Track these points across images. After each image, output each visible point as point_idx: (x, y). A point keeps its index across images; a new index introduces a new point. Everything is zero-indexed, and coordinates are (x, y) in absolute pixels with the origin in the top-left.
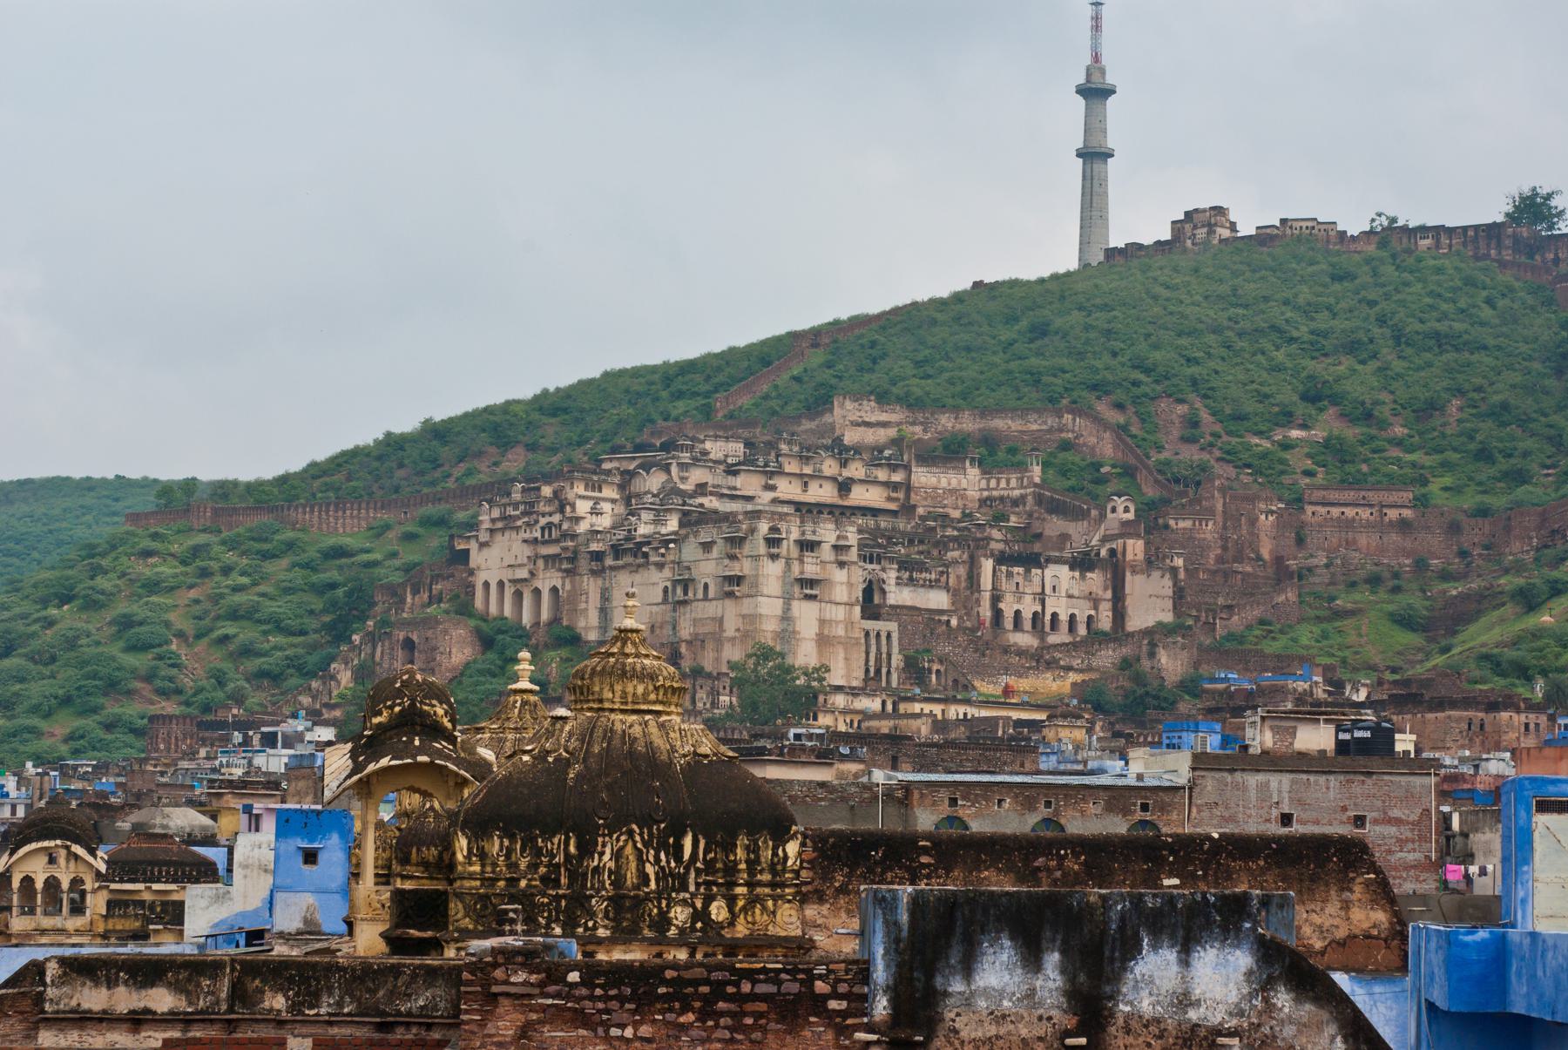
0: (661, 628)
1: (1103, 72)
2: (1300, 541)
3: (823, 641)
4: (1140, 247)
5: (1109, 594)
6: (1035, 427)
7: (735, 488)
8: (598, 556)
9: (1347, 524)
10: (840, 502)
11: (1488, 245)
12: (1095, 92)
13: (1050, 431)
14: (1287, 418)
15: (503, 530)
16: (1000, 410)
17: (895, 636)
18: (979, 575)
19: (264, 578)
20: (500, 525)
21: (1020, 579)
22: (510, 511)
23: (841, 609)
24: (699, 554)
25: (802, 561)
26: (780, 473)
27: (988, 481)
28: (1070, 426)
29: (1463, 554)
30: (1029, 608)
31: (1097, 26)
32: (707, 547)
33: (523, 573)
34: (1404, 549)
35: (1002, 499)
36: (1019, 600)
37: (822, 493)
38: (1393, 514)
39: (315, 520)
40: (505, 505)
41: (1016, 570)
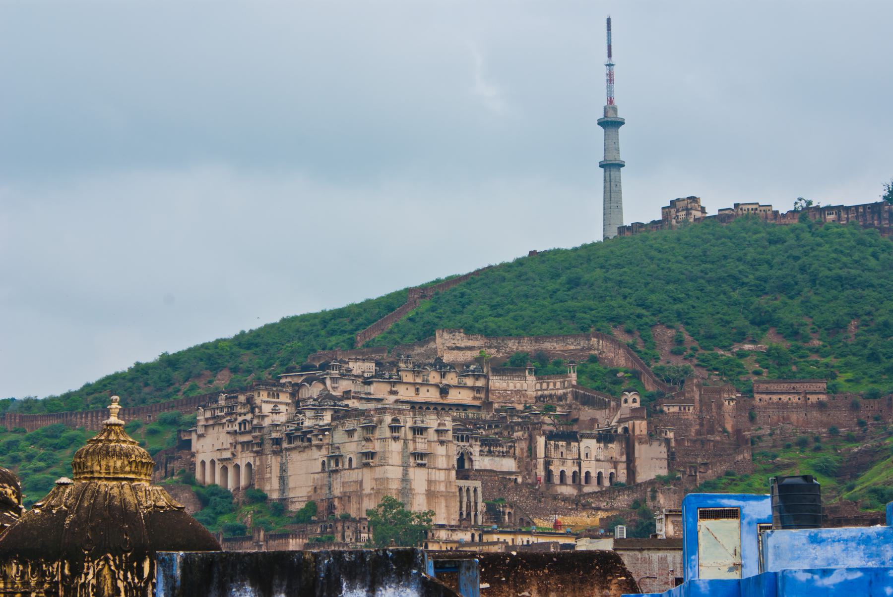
0: (321, 489)
1: (615, 110)
2: (752, 418)
3: (431, 495)
4: (641, 225)
5: (624, 458)
6: (572, 347)
7: (370, 394)
8: (277, 442)
9: (784, 406)
10: (441, 401)
11: (873, 218)
12: (610, 123)
13: (582, 349)
14: (742, 337)
15: (213, 426)
16: (548, 336)
17: (479, 490)
18: (535, 447)
19: (55, 463)
20: (211, 422)
21: (564, 450)
23: (442, 473)
24: (345, 438)
25: (414, 441)
26: (400, 382)
27: (541, 384)
28: (596, 346)
29: (861, 424)
30: (570, 469)
31: (610, 79)
32: (350, 433)
33: (227, 455)
34: (821, 422)
35: (551, 396)
36: (563, 464)
37: (430, 395)
38: (813, 398)
39: (89, 423)
40: (214, 409)
41: (560, 443)
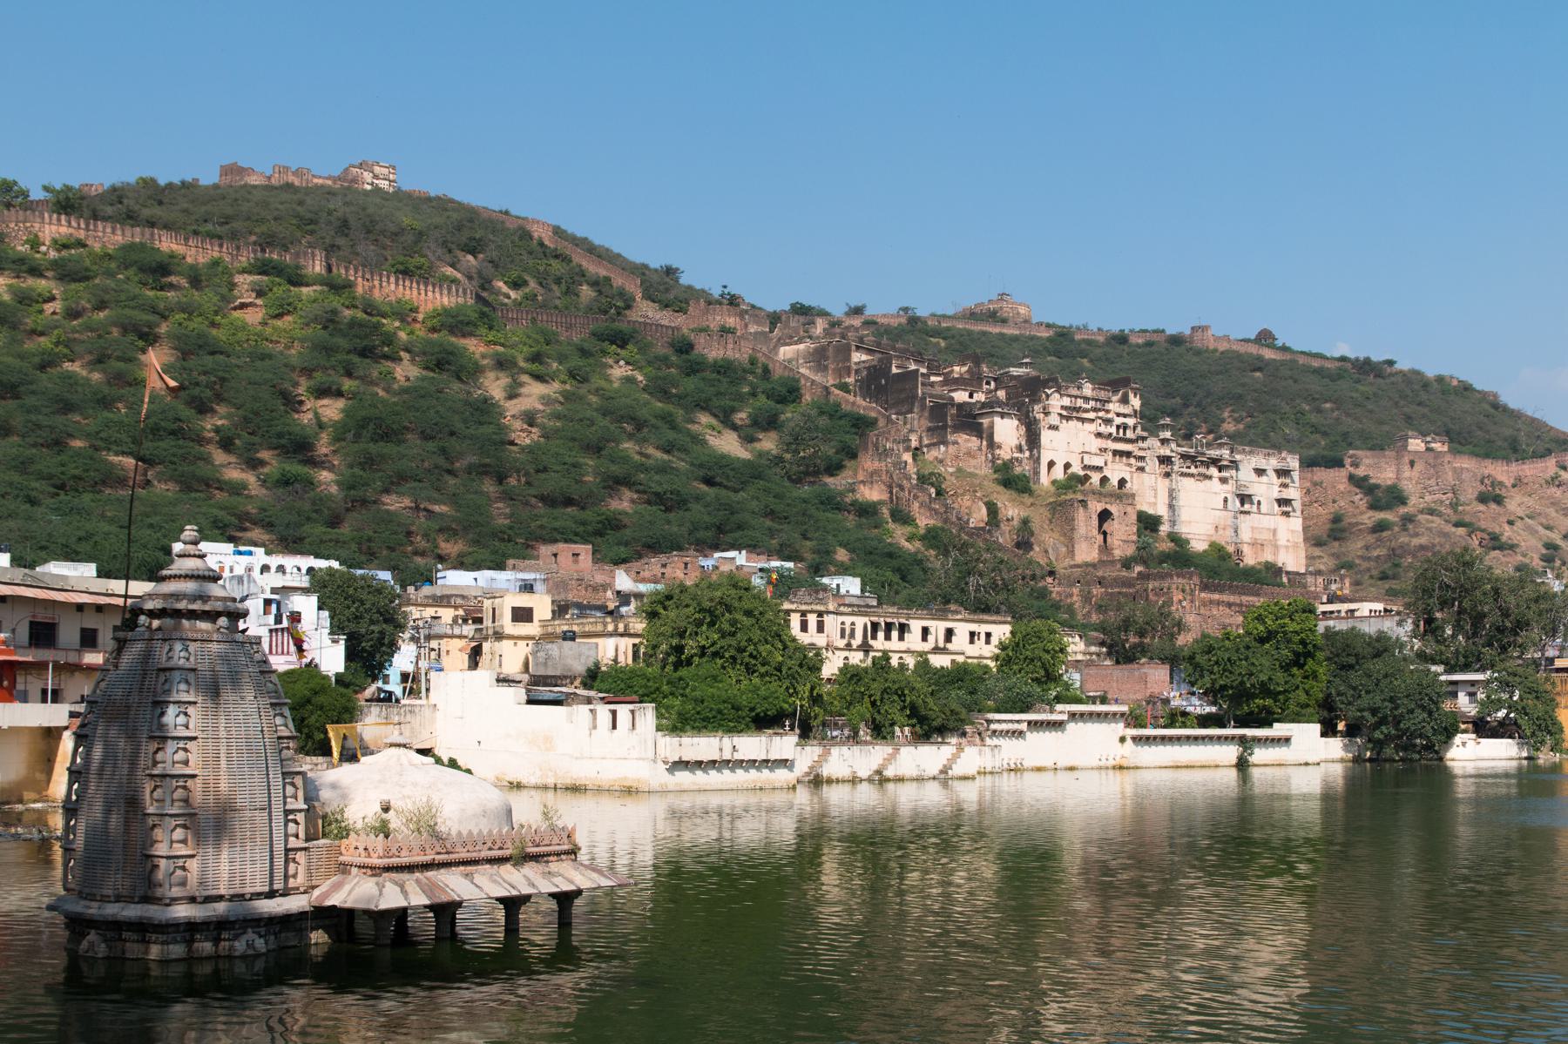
8: (1165, 460)
22: (1080, 402)
24: (1253, 476)
33: (1098, 461)
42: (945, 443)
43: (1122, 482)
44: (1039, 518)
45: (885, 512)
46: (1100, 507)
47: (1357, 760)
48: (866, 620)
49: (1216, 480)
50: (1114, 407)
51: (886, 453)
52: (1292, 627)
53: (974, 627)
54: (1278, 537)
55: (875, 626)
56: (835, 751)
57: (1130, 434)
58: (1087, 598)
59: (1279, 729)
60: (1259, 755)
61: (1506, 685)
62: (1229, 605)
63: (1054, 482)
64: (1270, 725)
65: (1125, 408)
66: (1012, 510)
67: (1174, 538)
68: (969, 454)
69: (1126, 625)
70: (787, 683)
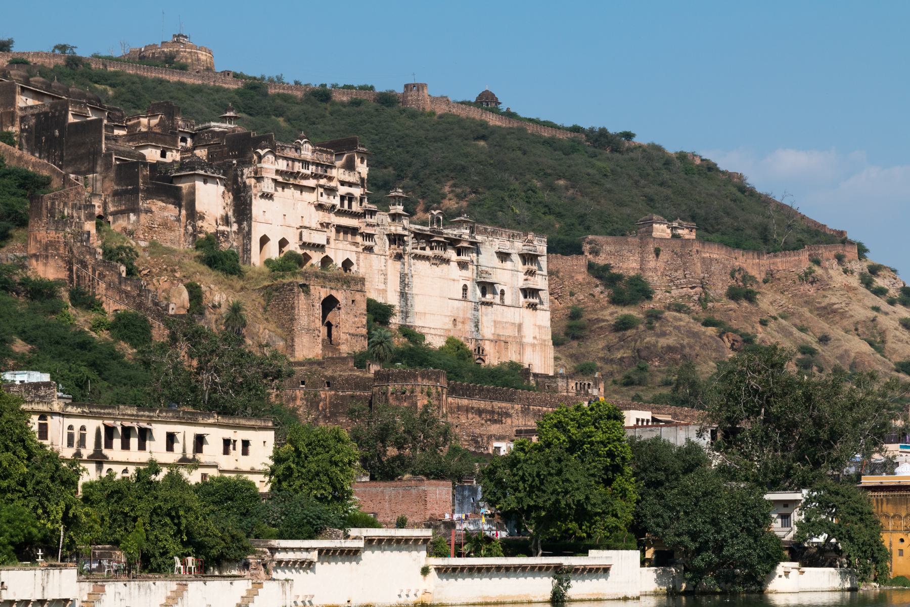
8: (396, 239)
22: (298, 167)
40: (294, 160)
42: (136, 211)
43: (347, 264)
44: (252, 304)
45: (65, 295)
46: (324, 293)
47: (672, 593)
48: (99, 423)
49: (453, 265)
50: (338, 173)
51: (64, 221)
52: (599, 436)
53: (229, 434)
54: (523, 335)
55: (110, 431)
56: (112, 588)
57: (356, 207)
58: (313, 402)
59: (596, 558)
60: (577, 588)
61: (824, 505)
62: (480, 412)
63: (268, 262)
64: (585, 552)
65: (351, 176)
66: (219, 295)
67: (407, 332)
68: (165, 225)
69: (383, 435)
70: (34, 502)
